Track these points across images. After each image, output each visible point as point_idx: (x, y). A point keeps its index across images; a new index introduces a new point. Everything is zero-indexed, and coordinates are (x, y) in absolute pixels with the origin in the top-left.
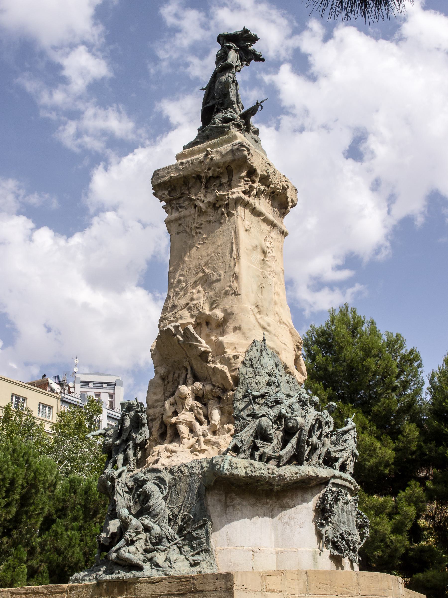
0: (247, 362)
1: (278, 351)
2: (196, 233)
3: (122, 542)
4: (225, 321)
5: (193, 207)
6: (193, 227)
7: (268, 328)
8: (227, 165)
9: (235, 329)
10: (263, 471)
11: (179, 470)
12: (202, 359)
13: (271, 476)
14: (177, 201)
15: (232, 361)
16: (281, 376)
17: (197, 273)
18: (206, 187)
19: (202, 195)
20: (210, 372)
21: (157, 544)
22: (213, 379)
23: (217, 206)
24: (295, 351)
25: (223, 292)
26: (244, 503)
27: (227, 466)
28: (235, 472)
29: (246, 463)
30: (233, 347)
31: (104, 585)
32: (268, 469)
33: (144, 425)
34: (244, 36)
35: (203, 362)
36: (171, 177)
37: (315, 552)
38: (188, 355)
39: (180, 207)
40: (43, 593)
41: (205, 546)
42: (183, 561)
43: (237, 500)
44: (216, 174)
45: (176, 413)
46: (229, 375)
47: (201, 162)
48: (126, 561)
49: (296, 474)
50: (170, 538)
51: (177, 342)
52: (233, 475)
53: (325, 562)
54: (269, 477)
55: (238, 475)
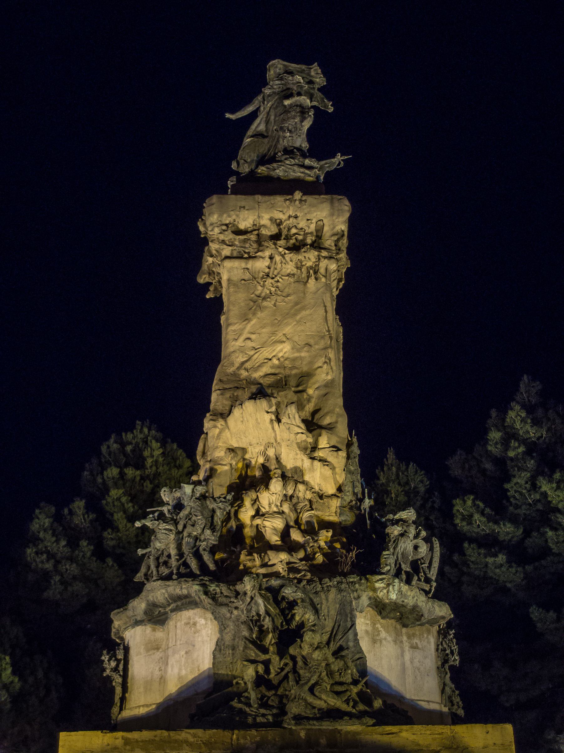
12: (299, 448)
26: (389, 639)
35: (298, 452)
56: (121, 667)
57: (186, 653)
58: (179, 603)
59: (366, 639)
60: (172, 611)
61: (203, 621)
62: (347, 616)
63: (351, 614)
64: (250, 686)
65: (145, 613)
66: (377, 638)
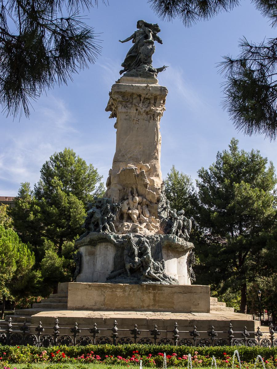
3: (149, 268)
5: (135, 109)
6: (135, 120)
11: (151, 238)
12: (144, 186)
14: (126, 103)
18: (143, 102)
20: (147, 192)
22: (147, 196)
26: (172, 255)
27: (176, 240)
31: (145, 286)
34: (155, 28)
36: (126, 91)
38: (137, 182)
39: (126, 107)
40: (109, 287)
44: (149, 97)
45: (129, 209)
48: (152, 277)
51: (134, 176)
52: (178, 244)
56: (79, 259)
57: (104, 257)
58: (102, 240)
59: (165, 255)
60: (99, 242)
61: (110, 247)
62: (159, 248)
63: (161, 247)
64: (128, 270)
65: (89, 242)
66: (169, 255)
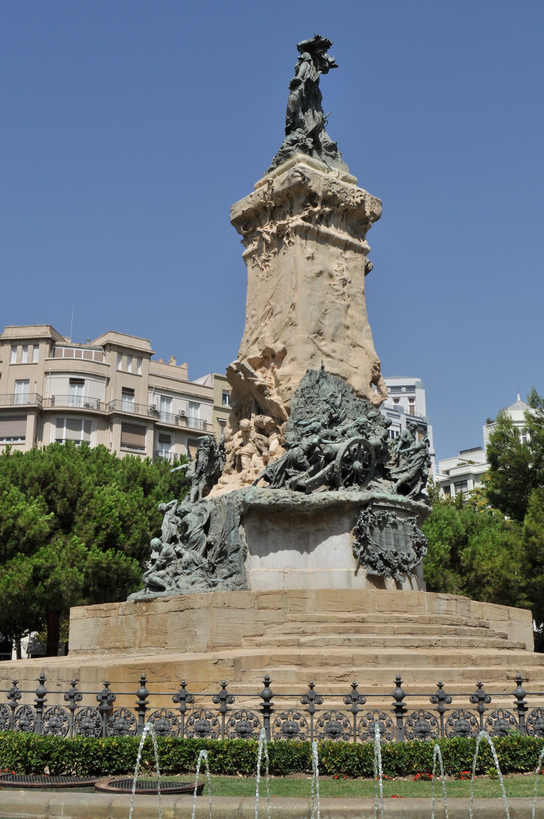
0: (298, 393)
1: (344, 376)
2: (265, 266)
4: (284, 352)
7: (333, 354)
8: (286, 193)
9: (293, 360)
10: (287, 500)
13: (295, 503)
15: (285, 393)
16: (348, 401)
17: (265, 306)
19: (268, 227)
21: (186, 568)
23: (280, 236)
24: (373, 372)
25: (284, 323)
28: (257, 501)
29: (269, 491)
30: (288, 378)
32: (293, 497)
33: (217, 458)
36: (243, 211)
37: (349, 572)
41: (238, 568)
42: (201, 582)
43: (270, 526)
46: (282, 406)
47: (265, 193)
49: (324, 499)
50: (197, 562)
53: (360, 581)
54: (294, 504)
55: (260, 504)
